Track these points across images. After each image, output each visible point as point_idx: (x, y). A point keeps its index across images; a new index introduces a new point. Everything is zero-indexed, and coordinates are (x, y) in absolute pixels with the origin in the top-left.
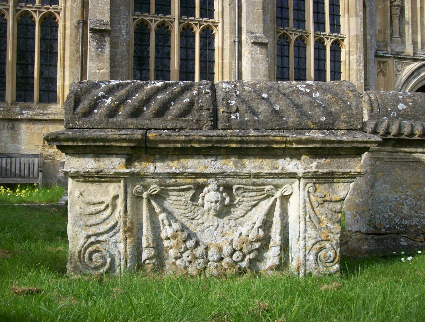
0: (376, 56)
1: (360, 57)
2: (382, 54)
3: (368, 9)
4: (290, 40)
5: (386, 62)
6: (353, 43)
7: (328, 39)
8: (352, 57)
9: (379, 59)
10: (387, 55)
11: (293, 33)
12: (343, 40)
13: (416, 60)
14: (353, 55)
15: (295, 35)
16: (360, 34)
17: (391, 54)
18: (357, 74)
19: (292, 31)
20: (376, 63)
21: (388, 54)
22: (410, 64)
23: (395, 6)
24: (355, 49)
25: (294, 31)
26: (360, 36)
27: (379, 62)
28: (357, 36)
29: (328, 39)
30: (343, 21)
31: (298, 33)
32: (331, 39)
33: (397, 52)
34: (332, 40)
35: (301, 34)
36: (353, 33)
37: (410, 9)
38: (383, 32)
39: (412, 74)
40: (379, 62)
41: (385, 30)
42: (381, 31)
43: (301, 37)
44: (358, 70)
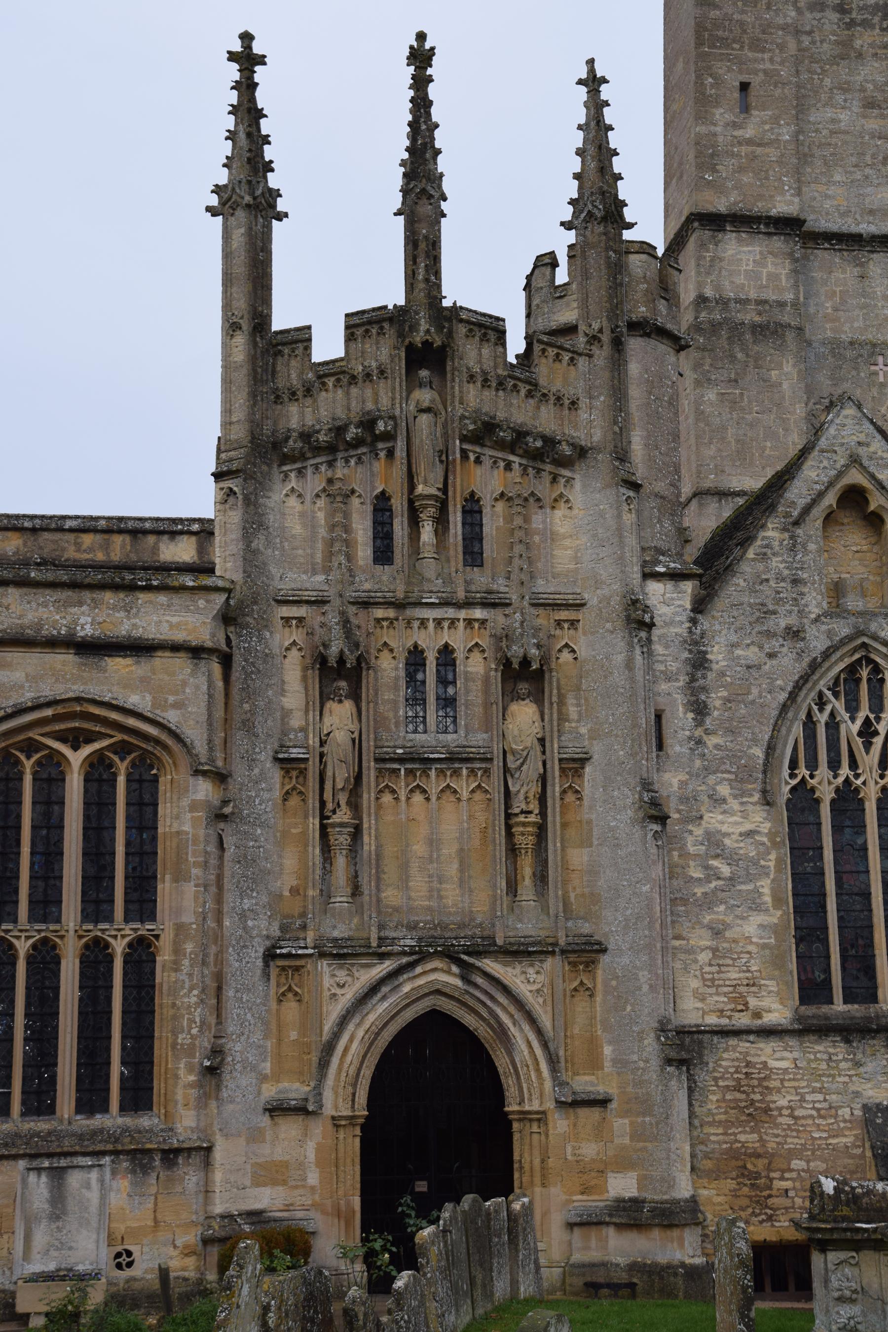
0: (270, 956)
3: (230, 851)
4: (16, 950)
5: (303, 967)
9: (281, 963)
11: (23, 935)
12: (157, 937)
13: (383, 956)
15: (28, 938)
16: (193, 920)
17: (314, 948)
19: (21, 931)
20: (274, 972)
21: (306, 948)
22: (374, 965)
23: (333, 825)
25: (26, 931)
26: (194, 926)
31: (35, 934)
33: (336, 940)
34: (127, 939)
35: (43, 934)
38: (301, 892)
39: (373, 989)
40: (283, 969)
42: (298, 890)
43: (45, 941)
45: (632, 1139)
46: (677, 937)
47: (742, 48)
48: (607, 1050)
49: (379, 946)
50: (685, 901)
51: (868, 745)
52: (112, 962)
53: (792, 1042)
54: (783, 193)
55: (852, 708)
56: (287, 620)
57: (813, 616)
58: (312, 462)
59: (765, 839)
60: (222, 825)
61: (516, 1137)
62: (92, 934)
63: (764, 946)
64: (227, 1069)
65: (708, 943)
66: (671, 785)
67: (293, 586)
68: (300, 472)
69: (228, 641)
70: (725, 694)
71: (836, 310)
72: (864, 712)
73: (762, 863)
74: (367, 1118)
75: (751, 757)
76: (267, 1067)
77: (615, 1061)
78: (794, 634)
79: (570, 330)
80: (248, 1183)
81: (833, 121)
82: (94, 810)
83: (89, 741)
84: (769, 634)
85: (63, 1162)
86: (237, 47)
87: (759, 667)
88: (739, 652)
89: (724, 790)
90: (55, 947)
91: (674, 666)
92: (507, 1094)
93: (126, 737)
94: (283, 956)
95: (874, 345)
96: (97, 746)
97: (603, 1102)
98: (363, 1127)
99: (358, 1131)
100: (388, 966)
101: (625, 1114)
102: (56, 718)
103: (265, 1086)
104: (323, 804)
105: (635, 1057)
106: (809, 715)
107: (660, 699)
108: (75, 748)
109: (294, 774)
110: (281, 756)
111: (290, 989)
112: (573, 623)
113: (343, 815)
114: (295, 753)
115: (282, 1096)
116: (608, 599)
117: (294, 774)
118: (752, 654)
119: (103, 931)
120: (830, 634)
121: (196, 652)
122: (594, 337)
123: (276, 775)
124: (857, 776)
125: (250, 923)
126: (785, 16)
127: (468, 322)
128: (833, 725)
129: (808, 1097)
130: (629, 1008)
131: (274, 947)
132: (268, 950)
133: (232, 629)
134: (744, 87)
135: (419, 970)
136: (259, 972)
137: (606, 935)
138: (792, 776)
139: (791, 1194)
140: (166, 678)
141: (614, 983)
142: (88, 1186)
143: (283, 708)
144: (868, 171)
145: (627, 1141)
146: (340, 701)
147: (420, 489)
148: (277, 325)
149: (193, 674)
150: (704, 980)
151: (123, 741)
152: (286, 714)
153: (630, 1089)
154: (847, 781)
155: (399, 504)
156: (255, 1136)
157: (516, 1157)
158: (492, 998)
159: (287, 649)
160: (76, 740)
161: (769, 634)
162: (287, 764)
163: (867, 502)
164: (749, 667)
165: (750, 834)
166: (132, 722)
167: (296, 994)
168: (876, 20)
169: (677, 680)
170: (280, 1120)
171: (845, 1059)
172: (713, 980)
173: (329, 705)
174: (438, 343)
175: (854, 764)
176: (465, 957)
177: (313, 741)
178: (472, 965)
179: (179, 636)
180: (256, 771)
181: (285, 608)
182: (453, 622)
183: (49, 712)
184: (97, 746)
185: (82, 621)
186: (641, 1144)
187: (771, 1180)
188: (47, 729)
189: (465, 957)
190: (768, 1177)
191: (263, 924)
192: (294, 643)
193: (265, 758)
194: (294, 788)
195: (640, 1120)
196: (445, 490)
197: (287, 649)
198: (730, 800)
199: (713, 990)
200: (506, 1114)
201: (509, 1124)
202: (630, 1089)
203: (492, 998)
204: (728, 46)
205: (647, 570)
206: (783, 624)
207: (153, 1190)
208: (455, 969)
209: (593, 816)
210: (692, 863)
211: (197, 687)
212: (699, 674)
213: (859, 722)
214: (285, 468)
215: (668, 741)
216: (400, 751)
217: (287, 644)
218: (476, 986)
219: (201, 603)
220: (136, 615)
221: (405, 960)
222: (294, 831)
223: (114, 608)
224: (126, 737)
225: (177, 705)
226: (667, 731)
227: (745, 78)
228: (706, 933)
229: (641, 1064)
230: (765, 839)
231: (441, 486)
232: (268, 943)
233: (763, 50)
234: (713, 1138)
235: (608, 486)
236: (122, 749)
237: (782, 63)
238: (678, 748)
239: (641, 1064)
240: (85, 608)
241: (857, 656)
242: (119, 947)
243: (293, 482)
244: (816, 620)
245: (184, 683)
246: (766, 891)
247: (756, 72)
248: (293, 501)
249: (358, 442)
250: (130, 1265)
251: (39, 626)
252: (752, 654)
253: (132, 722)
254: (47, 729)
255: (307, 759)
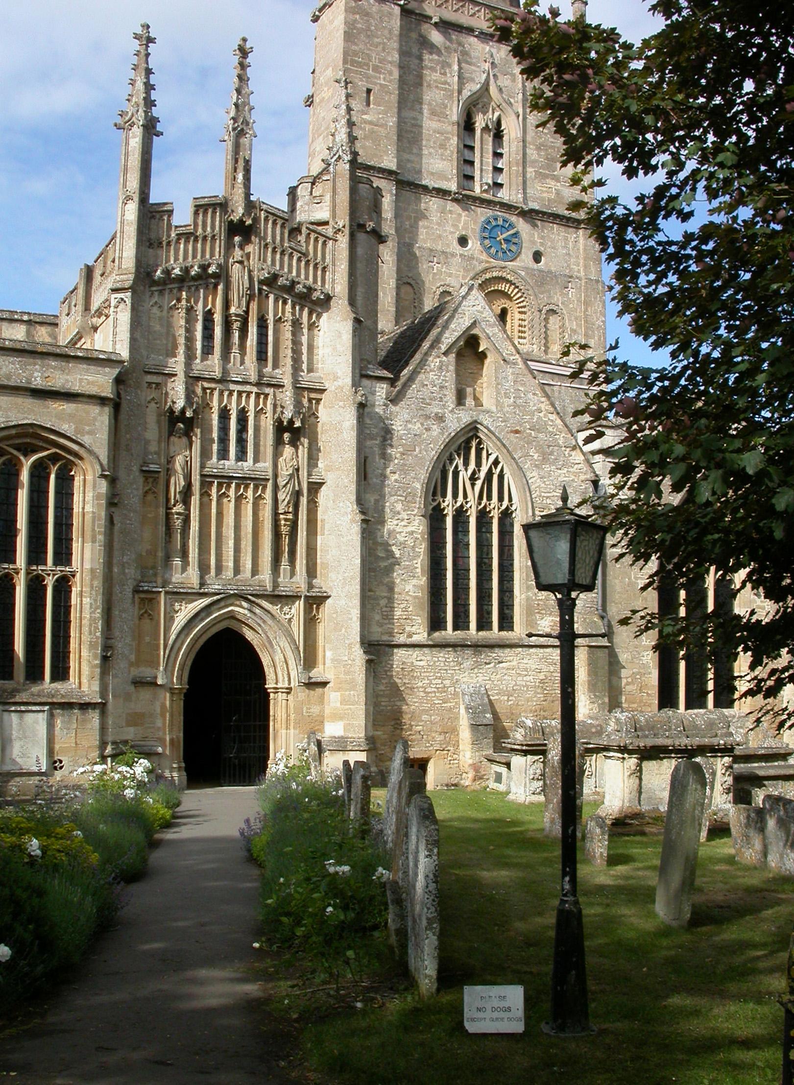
0: (136, 591)
1: (95, 600)
2: (146, 588)
3: (117, 527)
6: (87, 578)
7: (49, 575)
8: (84, 599)
9: (143, 596)
10: (154, 590)
12: (74, 576)
14: (86, 597)
18: (90, 625)
22: (196, 600)
24: (88, 589)
27: (142, 599)
28: (92, 571)
29: (49, 575)
30: (76, 546)
32: (54, 575)
36: (87, 566)
37: (197, 518)
39: (197, 615)
40: (142, 599)
41: (156, 551)
44: (92, 620)
45: (341, 704)
46: (370, 590)
47: (368, 70)
48: (329, 654)
49: (200, 589)
50: (374, 570)
51: (473, 485)
52: (46, 590)
53: (426, 650)
54: (388, 155)
55: (466, 464)
56: (150, 384)
57: (450, 409)
58: (170, 286)
59: (419, 536)
60: (113, 509)
61: (272, 702)
62: (35, 573)
63: (416, 597)
64: (115, 657)
65: (386, 594)
66: (370, 502)
67: (154, 363)
68: (161, 292)
69: (119, 395)
70: (401, 450)
71: (411, 227)
72: (472, 466)
73: (417, 550)
74: (188, 690)
75: (415, 489)
76: (133, 657)
77: (332, 660)
78: (440, 418)
79: (326, 223)
80: (124, 724)
81: (414, 119)
82: (35, 495)
83: (35, 451)
84: (428, 417)
85: (23, 708)
86: (139, 31)
87: (420, 435)
88: (409, 426)
89: (399, 507)
90: (12, 579)
91: (375, 431)
92: (267, 677)
93: (58, 451)
94: (143, 592)
95: (431, 250)
96: (41, 455)
97: (324, 684)
98: (186, 695)
99: (182, 697)
100: (206, 601)
101: (338, 690)
102: (17, 436)
103: (132, 669)
104: (168, 500)
105: (346, 658)
106: (444, 466)
107: (367, 450)
108: (25, 455)
109: (151, 480)
110: (144, 469)
111: (146, 612)
112: (318, 401)
113: (179, 508)
114: (153, 467)
115: (141, 675)
116: (341, 388)
117: (151, 480)
118: (417, 427)
119: (42, 570)
120: (459, 419)
121: (102, 401)
122: (339, 230)
123: (141, 480)
124: (467, 503)
125: (127, 571)
126: (393, 57)
127: (266, 211)
128: (456, 473)
129: (433, 682)
130: (343, 630)
131: (138, 586)
132: (134, 587)
133: (122, 387)
134: (369, 91)
135: (222, 604)
136: (130, 601)
137: (331, 588)
138: (434, 500)
139: (422, 733)
140: (84, 415)
141: (334, 616)
142: (36, 722)
143: (145, 439)
144: (432, 150)
145: (338, 704)
146: (180, 437)
147: (233, 310)
148: (152, 200)
149: (100, 414)
150: (383, 615)
151: (56, 453)
152: (147, 442)
153: (342, 676)
154: (485, 507)
155: (218, 317)
156: (127, 697)
157: (271, 713)
158: (264, 622)
159: (149, 402)
160: (28, 450)
161: (428, 417)
162: (148, 475)
163: (478, 345)
164: (415, 435)
165: (412, 533)
166: (62, 441)
167: (150, 615)
168: (438, 68)
169: (376, 440)
170: (140, 689)
171: (453, 661)
172: (387, 615)
173: (172, 439)
174: (249, 222)
175: (465, 496)
176: (250, 597)
177: (163, 460)
178: (254, 602)
179: (93, 390)
180: (132, 477)
181: (149, 376)
182: (249, 394)
183: (13, 432)
184: (41, 455)
185: (36, 374)
186: (347, 707)
187: (412, 726)
188: (10, 442)
189: (250, 597)
190: (410, 724)
191: (133, 571)
192: (153, 399)
193: (135, 469)
194: (150, 490)
195: (347, 693)
196: (247, 312)
197: (149, 402)
198: (402, 512)
199: (387, 621)
200: (267, 689)
201: (268, 694)
202: (342, 676)
203: (264, 622)
204: (361, 67)
205: (364, 372)
206: (436, 410)
207: (75, 726)
208: (245, 604)
209: (326, 517)
210: (379, 548)
211: (102, 422)
212: (388, 437)
213: (470, 472)
214: (154, 289)
215: (370, 476)
216: (215, 470)
217: (149, 399)
218: (255, 613)
219: (107, 370)
220: (68, 375)
221: (215, 598)
222: (149, 515)
223: (55, 368)
224: (58, 451)
225: (90, 433)
226: (369, 470)
227: (370, 86)
228: (384, 588)
229: (350, 662)
230: (419, 536)
231: (244, 309)
232: (135, 584)
233: (380, 73)
234: (383, 704)
235: (346, 320)
236: (54, 458)
237: (390, 81)
238: (375, 480)
239: (350, 662)
240: (37, 367)
241: (471, 434)
242: (50, 582)
243: (156, 298)
244: (452, 411)
245: (95, 419)
246: (419, 565)
247: (376, 84)
248: (155, 310)
249: (198, 277)
250: (61, 768)
251: (9, 377)
252: (417, 427)
253: (62, 441)
254: (10, 442)
255: (159, 472)
